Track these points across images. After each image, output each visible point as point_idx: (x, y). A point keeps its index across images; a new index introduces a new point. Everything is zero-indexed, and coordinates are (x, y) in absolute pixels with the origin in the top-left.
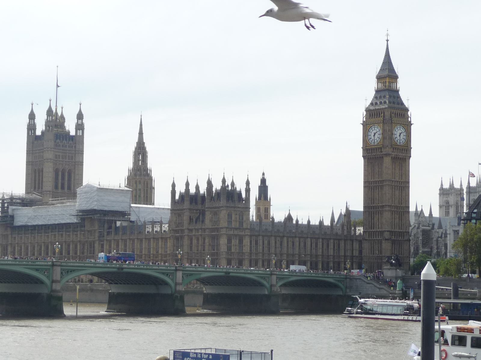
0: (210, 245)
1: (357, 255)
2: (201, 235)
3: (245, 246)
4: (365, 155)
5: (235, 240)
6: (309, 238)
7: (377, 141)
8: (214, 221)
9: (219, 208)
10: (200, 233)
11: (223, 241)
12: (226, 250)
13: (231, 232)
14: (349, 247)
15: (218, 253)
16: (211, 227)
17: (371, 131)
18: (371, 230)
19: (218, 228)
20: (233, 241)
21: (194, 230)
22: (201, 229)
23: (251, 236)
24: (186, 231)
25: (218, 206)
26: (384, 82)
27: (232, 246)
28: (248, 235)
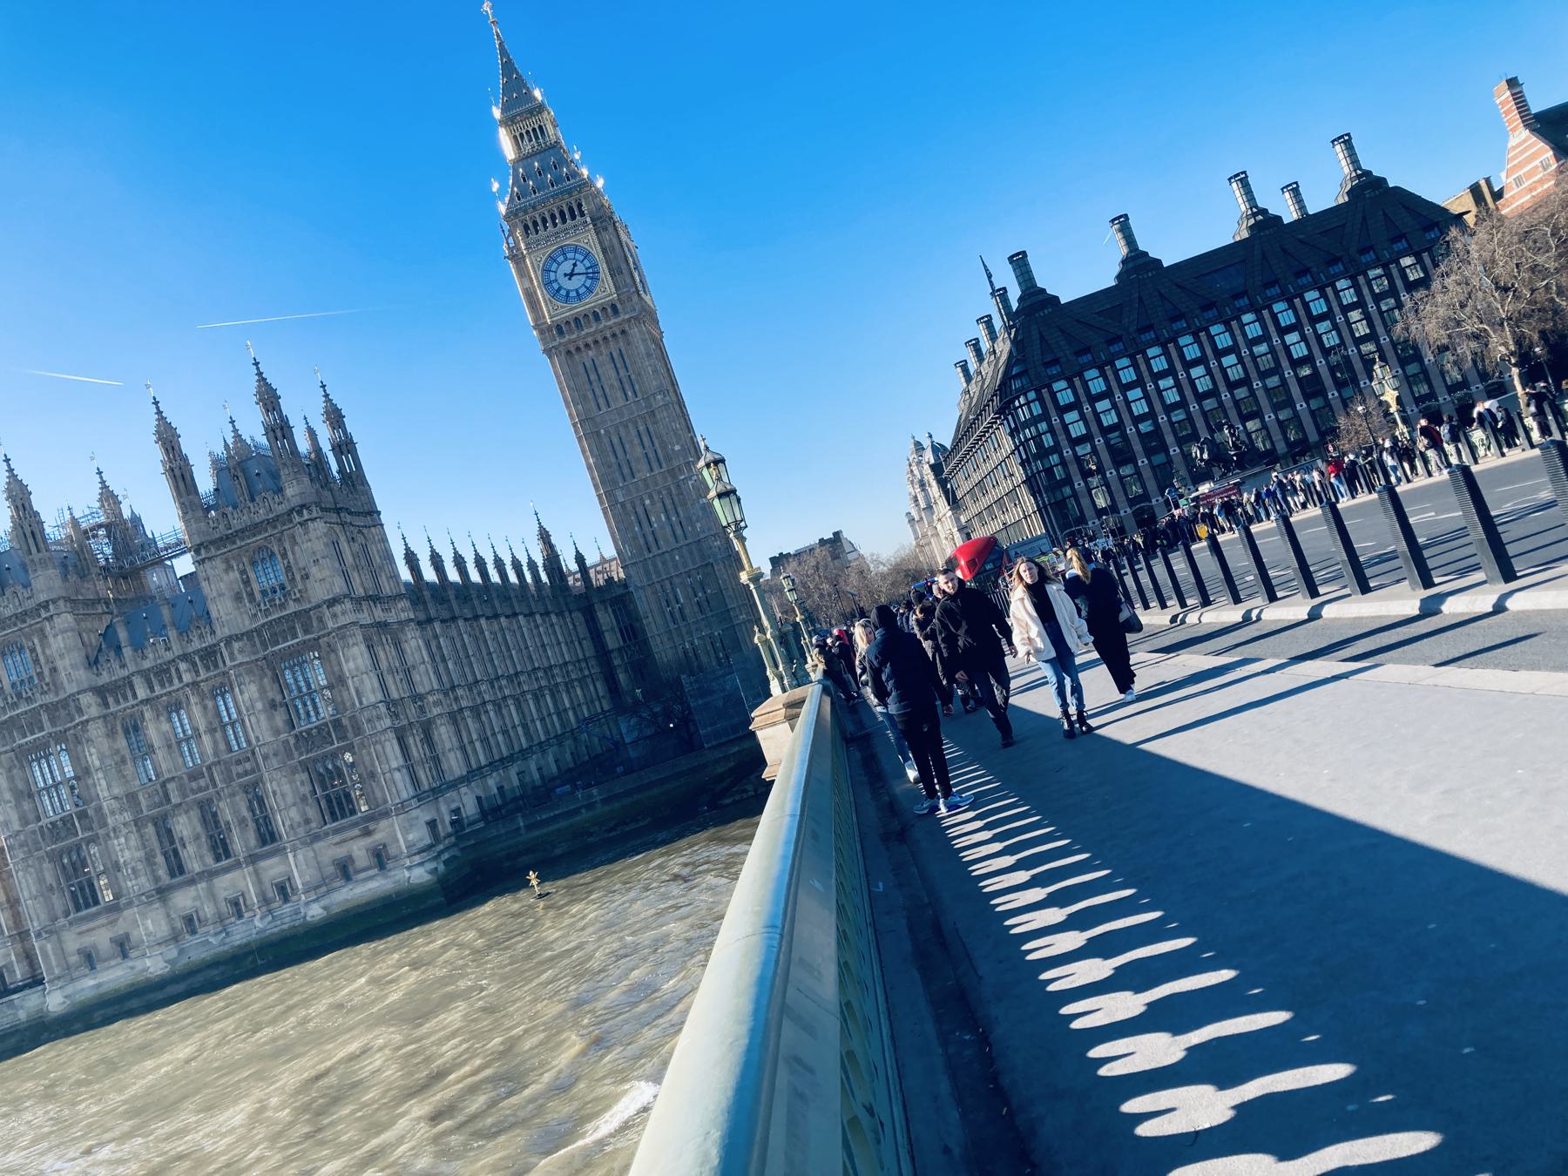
0: (273, 705)
1: (617, 646)
2: (195, 685)
3: (414, 667)
4: (555, 344)
5: (387, 647)
6: (521, 613)
7: (588, 288)
8: (264, 593)
9: (272, 522)
10: (187, 678)
11: (355, 658)
12: (380, 696)
13: (365, 618)
14: (583, 631)
15: (345, 722)
16: (247, 625)
17: (553, 269)
18: (651, 555)
19: (307, 611)
20: (382, 655)
21: (138, 683)
22: (185, 657)
23: (419, 623)
24: (87, 700)
25: (271, 516)
26: (534, 130)
27: (385, 673)
28: (412, 620)
